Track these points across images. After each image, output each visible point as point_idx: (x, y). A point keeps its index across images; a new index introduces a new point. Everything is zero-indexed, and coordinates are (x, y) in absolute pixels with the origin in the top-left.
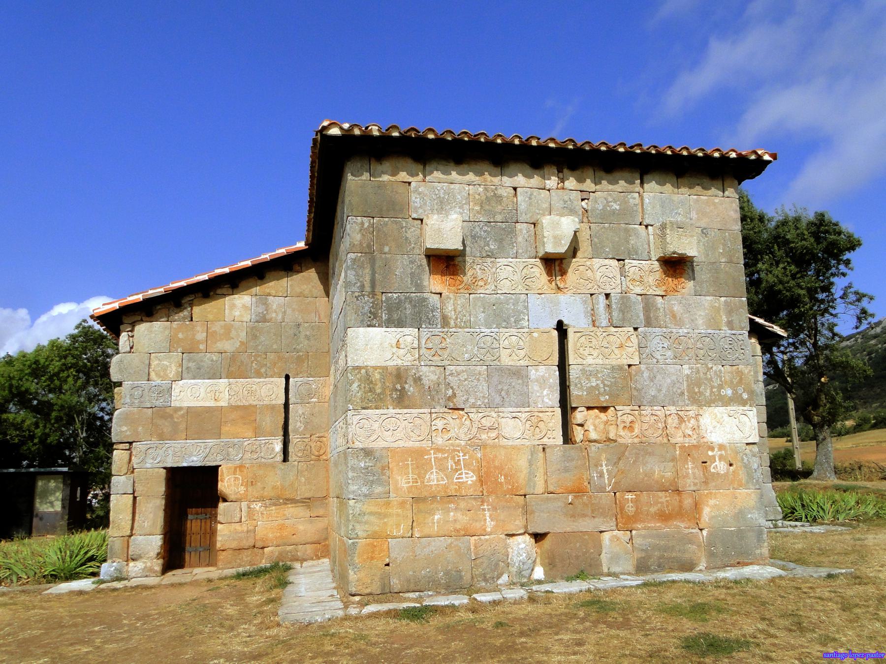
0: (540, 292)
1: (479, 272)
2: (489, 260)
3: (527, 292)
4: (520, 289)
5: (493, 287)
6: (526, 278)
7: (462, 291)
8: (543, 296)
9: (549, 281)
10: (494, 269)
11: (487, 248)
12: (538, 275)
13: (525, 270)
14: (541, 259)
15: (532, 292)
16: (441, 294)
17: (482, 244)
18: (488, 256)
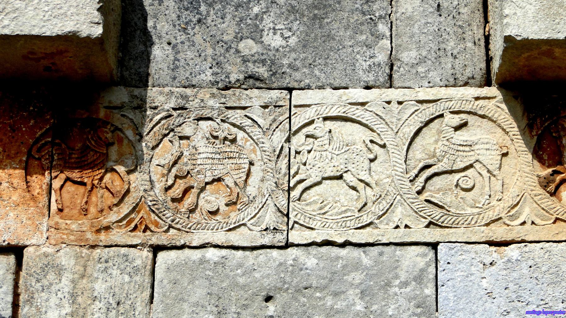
0: (498, 232)
1: (205, 149)
2: (256, 98)
3: (432, 235)
4: (405, 219)
5: (270, 218)
6: (428, 172)
7: (118, 235)
8: (512, 251)
9: (545, 183)
10: (279, 138)
11: (248, 46)
12: (491, 158)
13: (428, 138)
14: (503, 85)
15: (459, 234)
16: (17, 251)
17: (228, 29)
18: (253, 81)
